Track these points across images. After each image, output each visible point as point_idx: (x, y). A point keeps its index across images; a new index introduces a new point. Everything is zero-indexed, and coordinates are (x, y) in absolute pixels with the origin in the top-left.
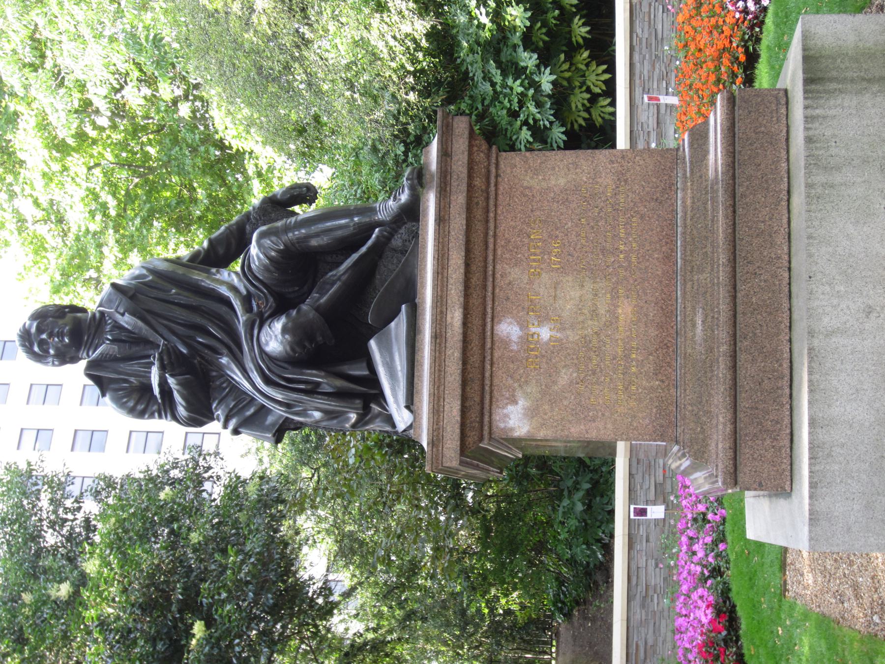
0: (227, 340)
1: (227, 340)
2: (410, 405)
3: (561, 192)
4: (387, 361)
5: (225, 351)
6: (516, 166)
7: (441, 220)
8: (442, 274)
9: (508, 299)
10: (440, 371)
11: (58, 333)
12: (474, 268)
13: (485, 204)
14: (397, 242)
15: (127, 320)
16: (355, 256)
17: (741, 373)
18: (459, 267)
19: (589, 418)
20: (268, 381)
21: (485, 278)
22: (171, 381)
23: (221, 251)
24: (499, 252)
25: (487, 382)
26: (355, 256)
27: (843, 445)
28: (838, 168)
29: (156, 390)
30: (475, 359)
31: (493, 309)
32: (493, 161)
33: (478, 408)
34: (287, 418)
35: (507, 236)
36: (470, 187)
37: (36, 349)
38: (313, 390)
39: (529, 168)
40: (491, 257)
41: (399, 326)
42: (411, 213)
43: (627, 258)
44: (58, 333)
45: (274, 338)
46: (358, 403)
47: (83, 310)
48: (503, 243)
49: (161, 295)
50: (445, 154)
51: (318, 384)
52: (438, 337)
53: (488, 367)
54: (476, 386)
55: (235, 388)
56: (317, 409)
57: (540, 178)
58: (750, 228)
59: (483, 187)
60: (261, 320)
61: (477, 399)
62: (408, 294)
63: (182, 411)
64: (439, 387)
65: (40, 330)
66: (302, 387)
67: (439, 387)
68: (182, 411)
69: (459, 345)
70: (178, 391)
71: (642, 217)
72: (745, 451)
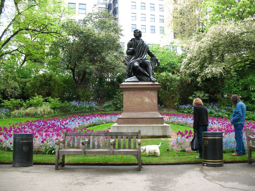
7: (148, 85)
11: (138, 34)
14: (149, 78)
16: (147, 73)
17: (131, 119)
23: (151, 54)
26: (147, 73)
28: (153, 129)
30: (132, 89)
36: (152, 88)
38: (130, 69)
42: (151, 81)
44: (138, 34)
45: (136, 64)
47: (141, 37)
50: (156, 84)
52: (134, 85)
55: (131, 58)
60: (138, 61)
62: (140, 80)
63: (128, 51)
65: (138, 32)
72: (121, 119)
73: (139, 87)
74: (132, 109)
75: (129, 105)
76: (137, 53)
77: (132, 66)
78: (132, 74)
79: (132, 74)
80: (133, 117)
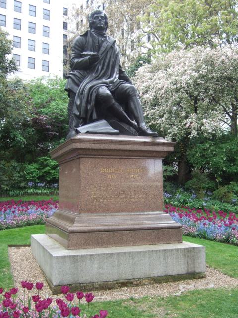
0: (100, 75)
1: (100, 75)
2: (88, 132)
4: (102, 125)
5: (96, 75)
7: (145, 143)
9: (121, 162)
15: (105, 45)
16: (127, 116)
20: (91, 88)
21: (127, 156)
22: (87, 57)
24: (135, 160)
25: (97, 156)
26: (127, 116)
27: (86, 265)
28: (164, 259)
29: (84, 53)
30: (104, 153)
31: (119, 158)
33: (89, 153)
34: (76, 94)
37: (95, 16)
38: (88, 102)
41: (110, 129)
42: (142, 133)
43: (133, 198)
45: (105, 91)
46: (84, 116)
49: (112, 55)
51: (90, 104)
52: (111, 142)
53: (101, 156)
54: (96, 153)
55: (84, 77)
56: (81, 103)
58: (145, 234)
61: (92, 153)
62: (123, 132)
63: (76, 60)
65: (102, 17)
66: (89, 99)
68: (76, 60)
69: (109, 148)
70: (83, 60)
71: (145, 202)
72: (79, 235)
73: (102, 146)
74: (102, 205)
75: (95, 194)
76: (100, 67)
77: (94, 95)
78: (95, 116)
79: (95, 116)
80: (110, 227)
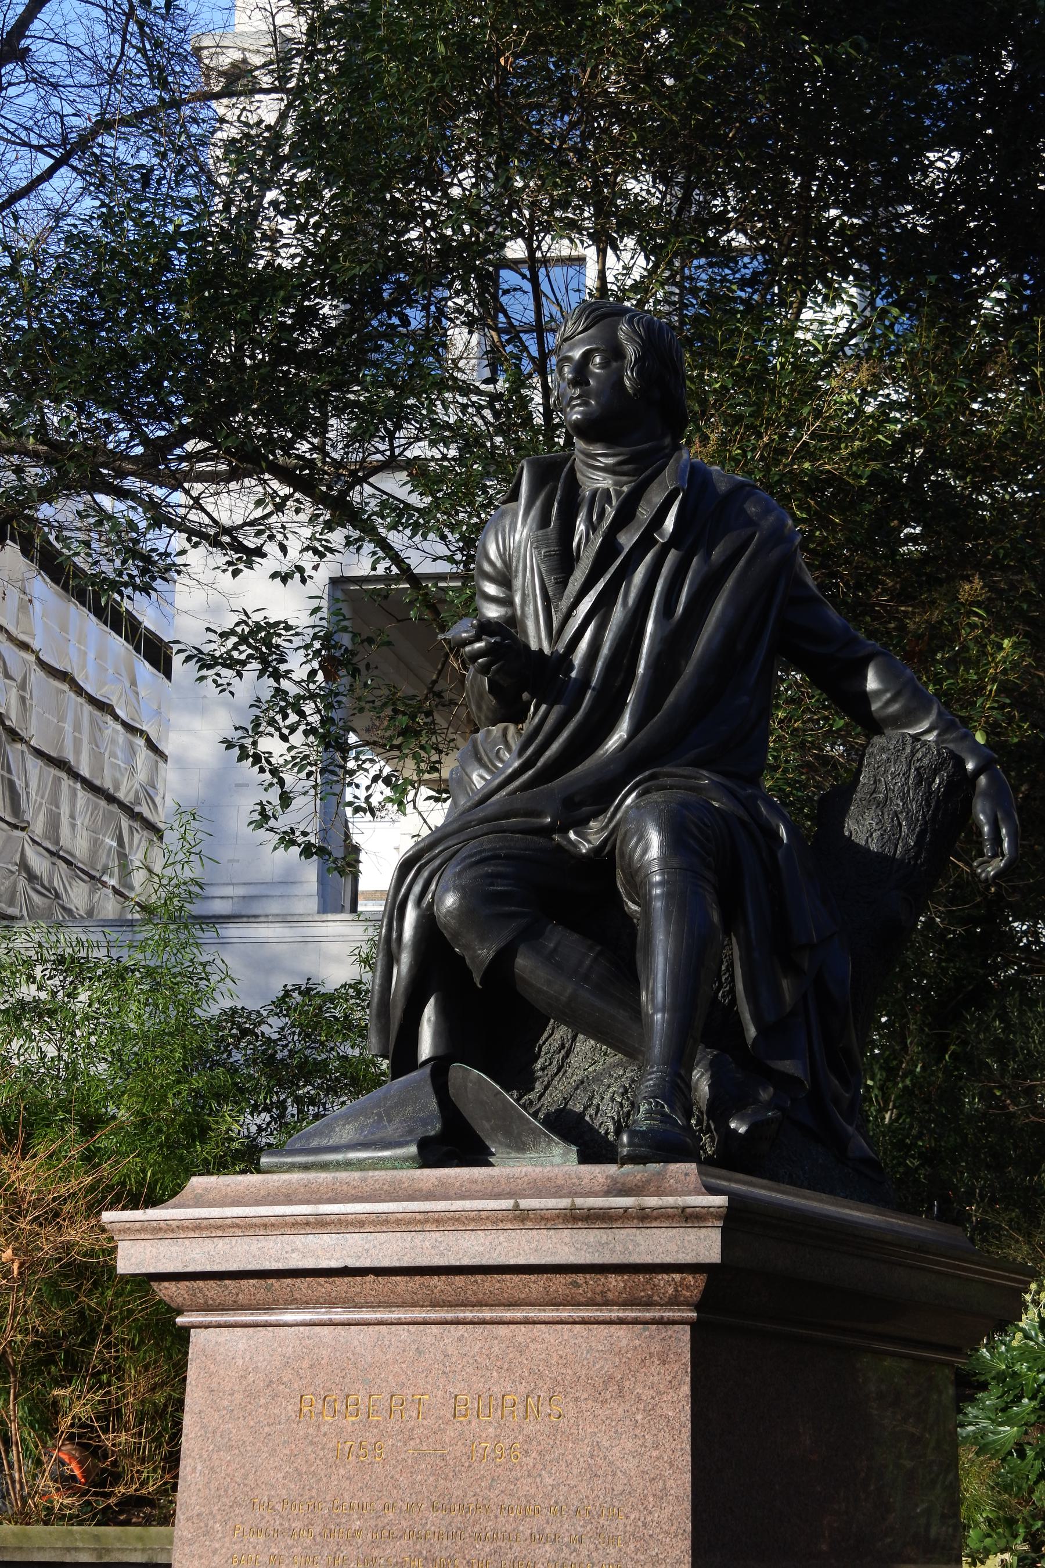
3: (611, 1463)
6: (664, 1363)
8: (426, 1221)
10: (265, 1226)
12: (459, 1280)
13: (583, 1300)
18: (442, 1254)
19: (211, 1523)
24: (503, 1330)
32: (667, 1315)
35: (532, 1346)
39: (659, 1393)
40: (487, 1314)
48: (520, 1339)
51: (398, 961)
57: (639, 1417)
59: (610, 1296)
64: (238, 1226)
67: (238, 1226)
